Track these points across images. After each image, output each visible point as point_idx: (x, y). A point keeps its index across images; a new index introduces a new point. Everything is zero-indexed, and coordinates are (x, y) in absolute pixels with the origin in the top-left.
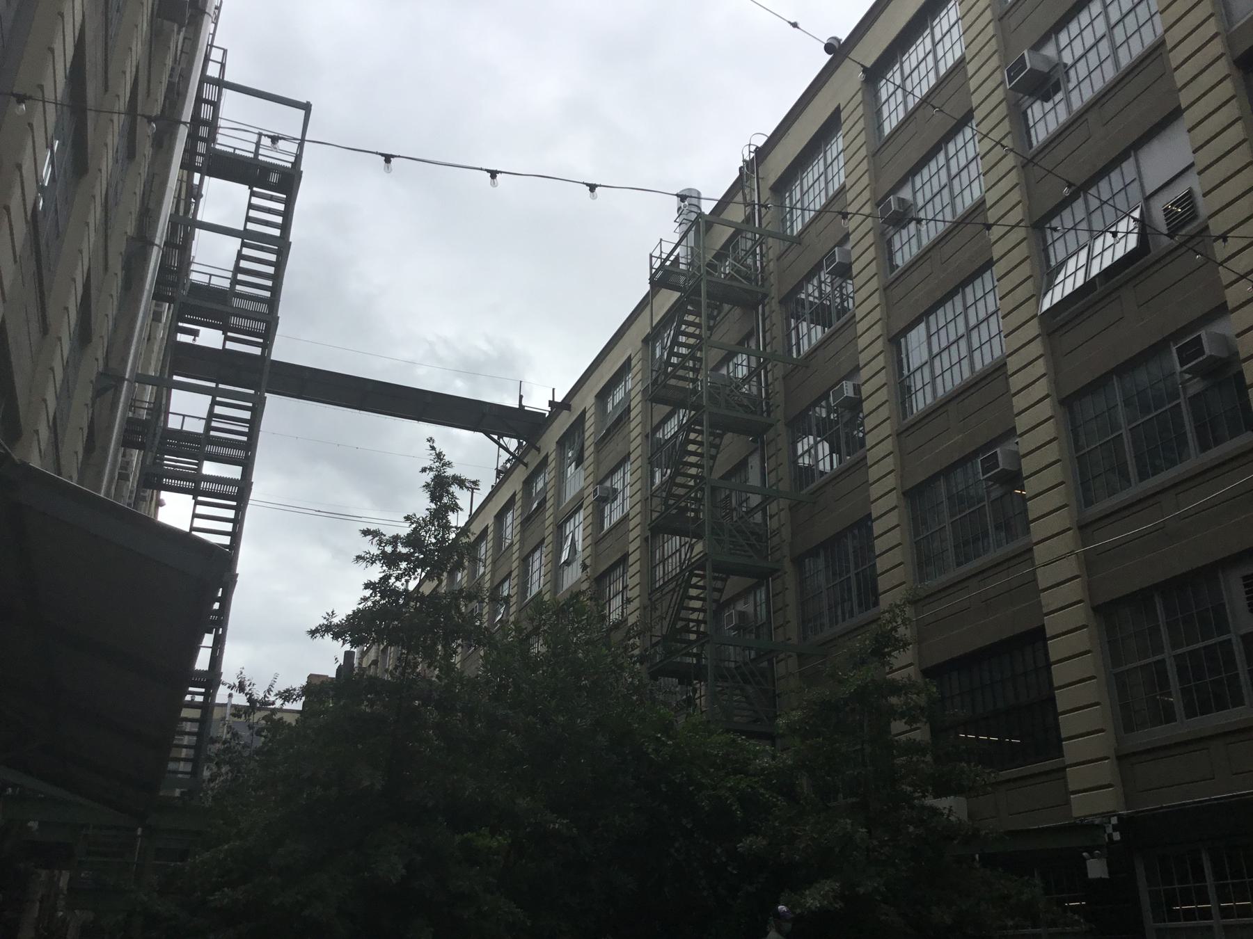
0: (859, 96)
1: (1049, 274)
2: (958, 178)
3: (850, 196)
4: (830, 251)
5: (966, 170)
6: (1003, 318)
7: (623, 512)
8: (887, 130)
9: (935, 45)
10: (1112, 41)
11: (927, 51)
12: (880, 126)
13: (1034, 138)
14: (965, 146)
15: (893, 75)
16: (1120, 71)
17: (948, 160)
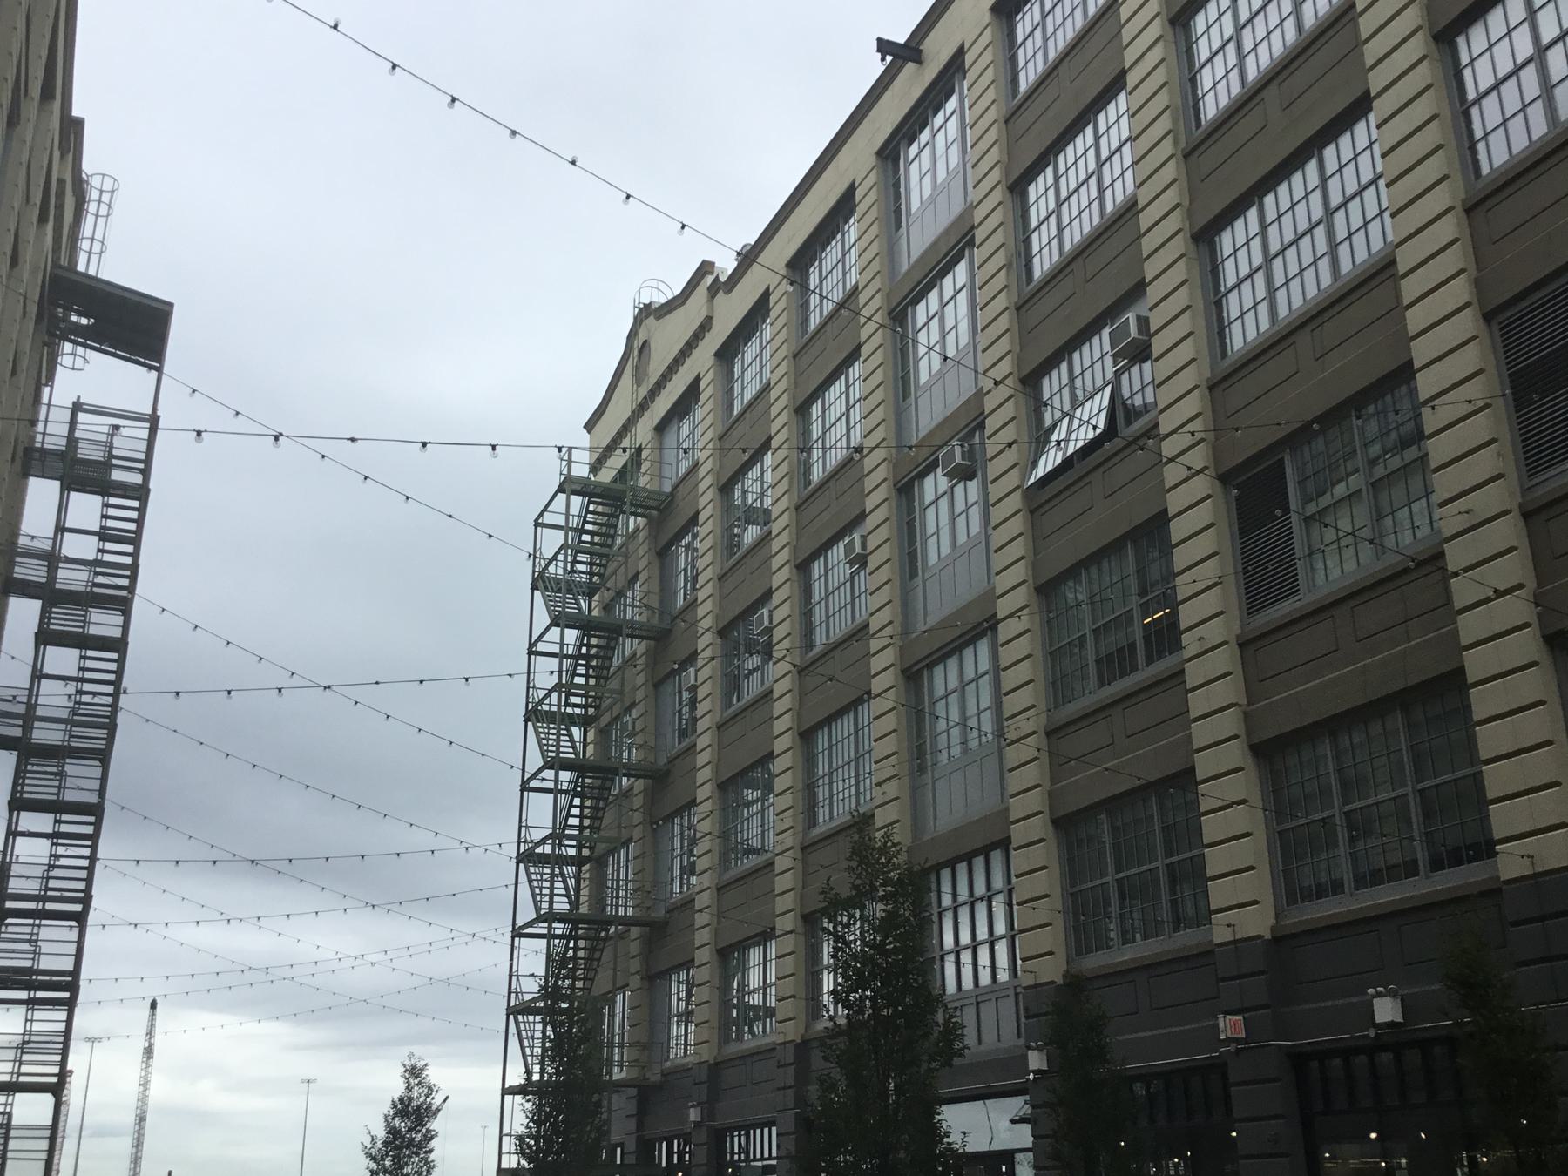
0: (988, 33)
1: (1041, 439)
2: (1108, 164)
3: (863, 298)
4: (966, 235)
5: (1118, 154)
6: (870, 574)
7: (685, 599)
8: (1023, 87)
9: (1044, 16)
10: (1239, 48)
11: (1035, 24)
12: (1014, 81)
13: (1202, 116)
14: (1115, 119)
15: (1023, 17)
16: (1105, 218)
17: (1097, 138)
